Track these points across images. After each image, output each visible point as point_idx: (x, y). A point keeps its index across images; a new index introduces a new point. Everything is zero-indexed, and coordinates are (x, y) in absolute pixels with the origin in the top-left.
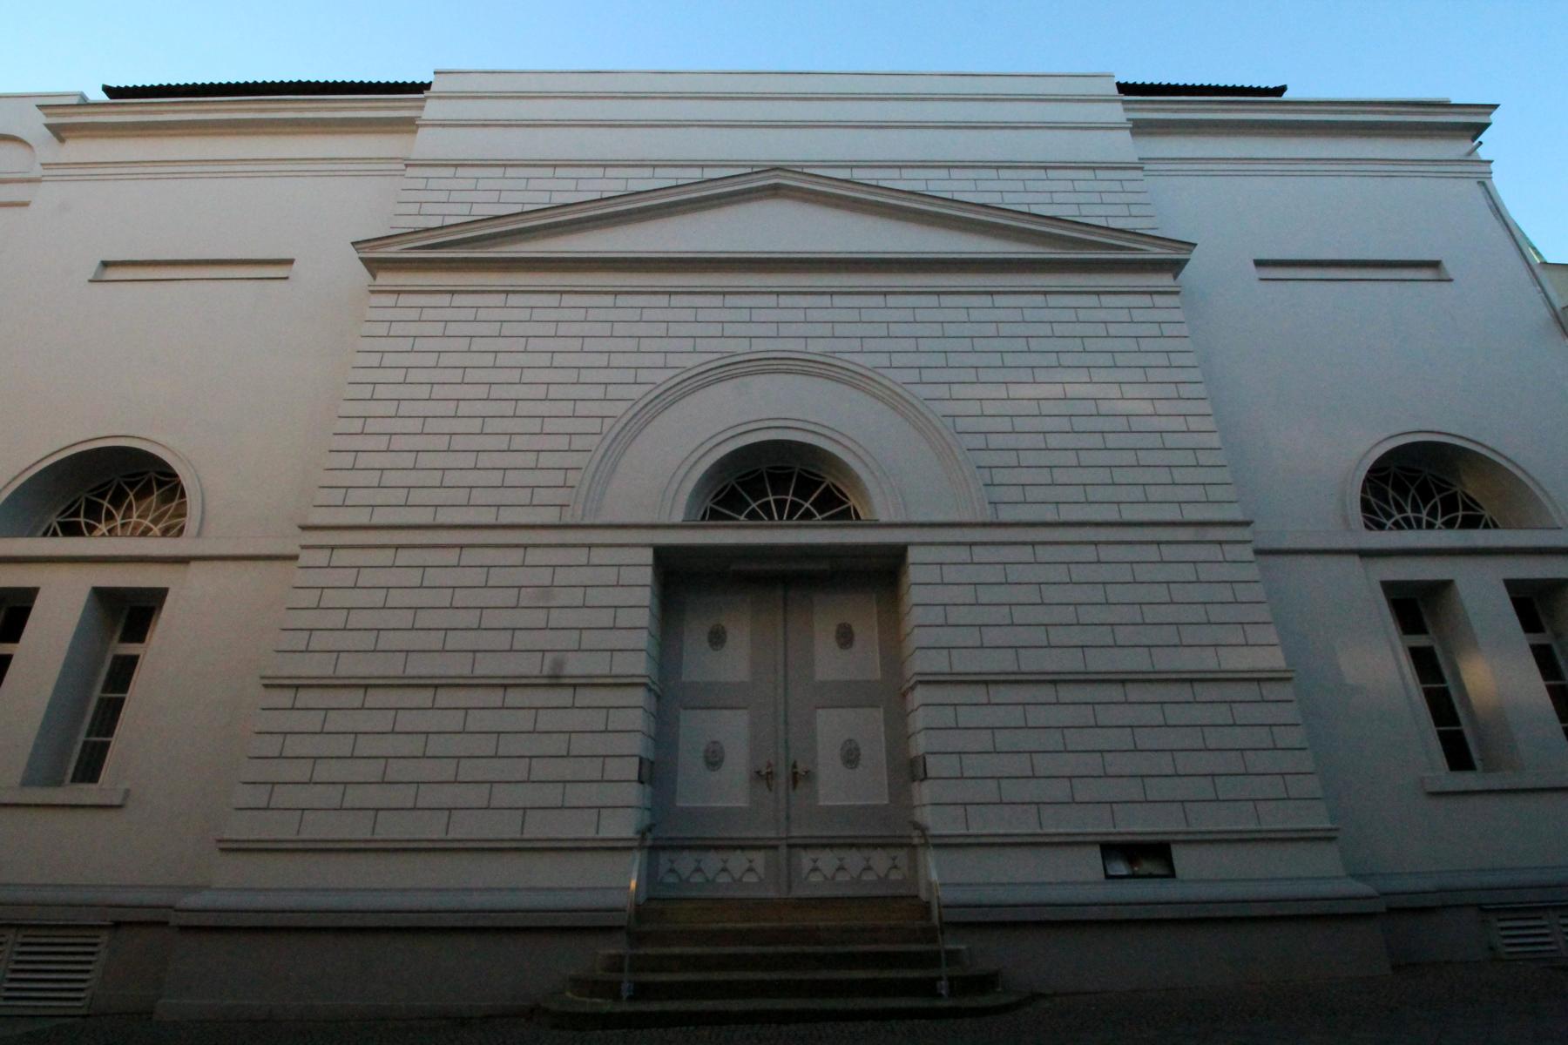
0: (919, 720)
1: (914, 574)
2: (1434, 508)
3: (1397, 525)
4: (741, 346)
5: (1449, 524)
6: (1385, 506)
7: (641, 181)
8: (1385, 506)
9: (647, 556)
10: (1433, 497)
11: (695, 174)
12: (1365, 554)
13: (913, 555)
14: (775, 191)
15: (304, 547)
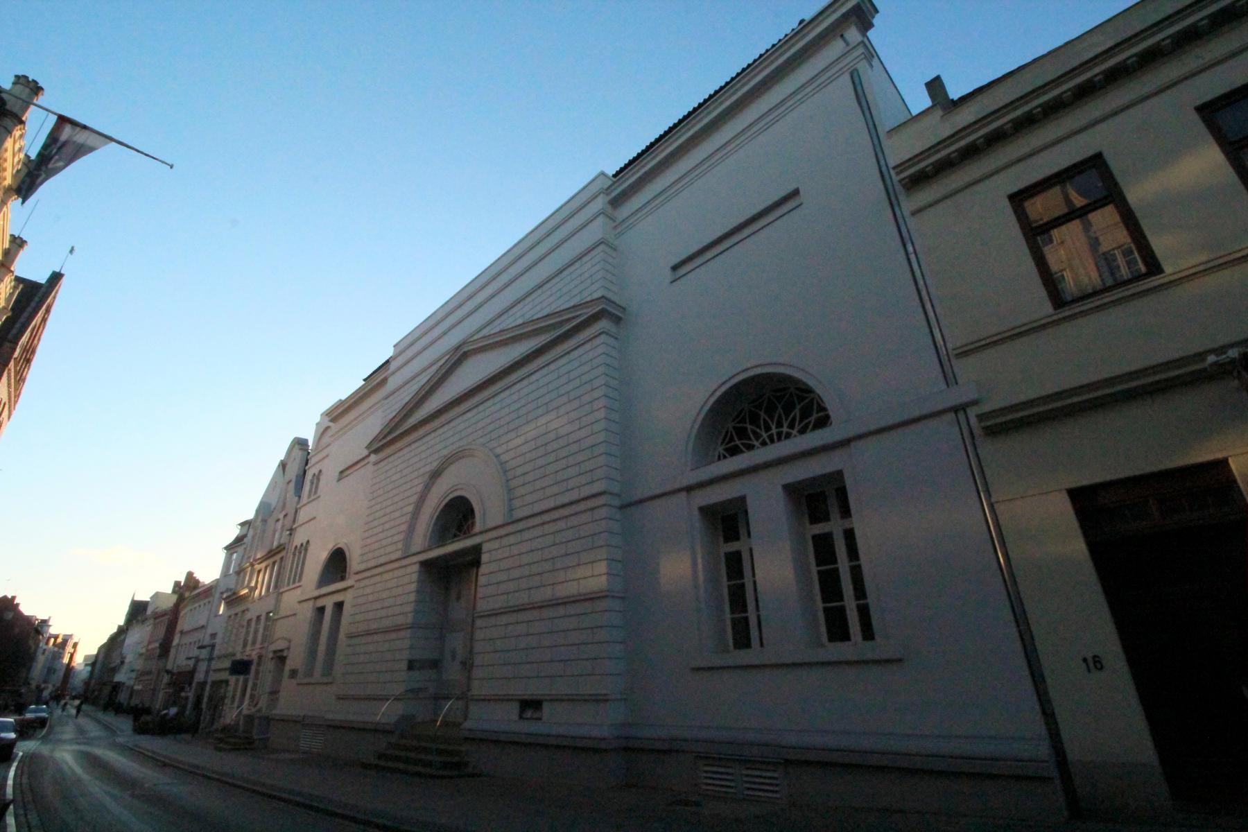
0: (479, 635)
1: (485, 558)
2: (794, 419)
3: (764, 444)
4: (445, 452)
5: (802, 431)
6: (784, 418)
7: (423, 379)
8: (784, 418)
9: (416, 568)
10: (746, 429)
11: (435, 368)
12: (689, 489)
13: (485, 547)
14: (465, 356)
15: (356, 581)
